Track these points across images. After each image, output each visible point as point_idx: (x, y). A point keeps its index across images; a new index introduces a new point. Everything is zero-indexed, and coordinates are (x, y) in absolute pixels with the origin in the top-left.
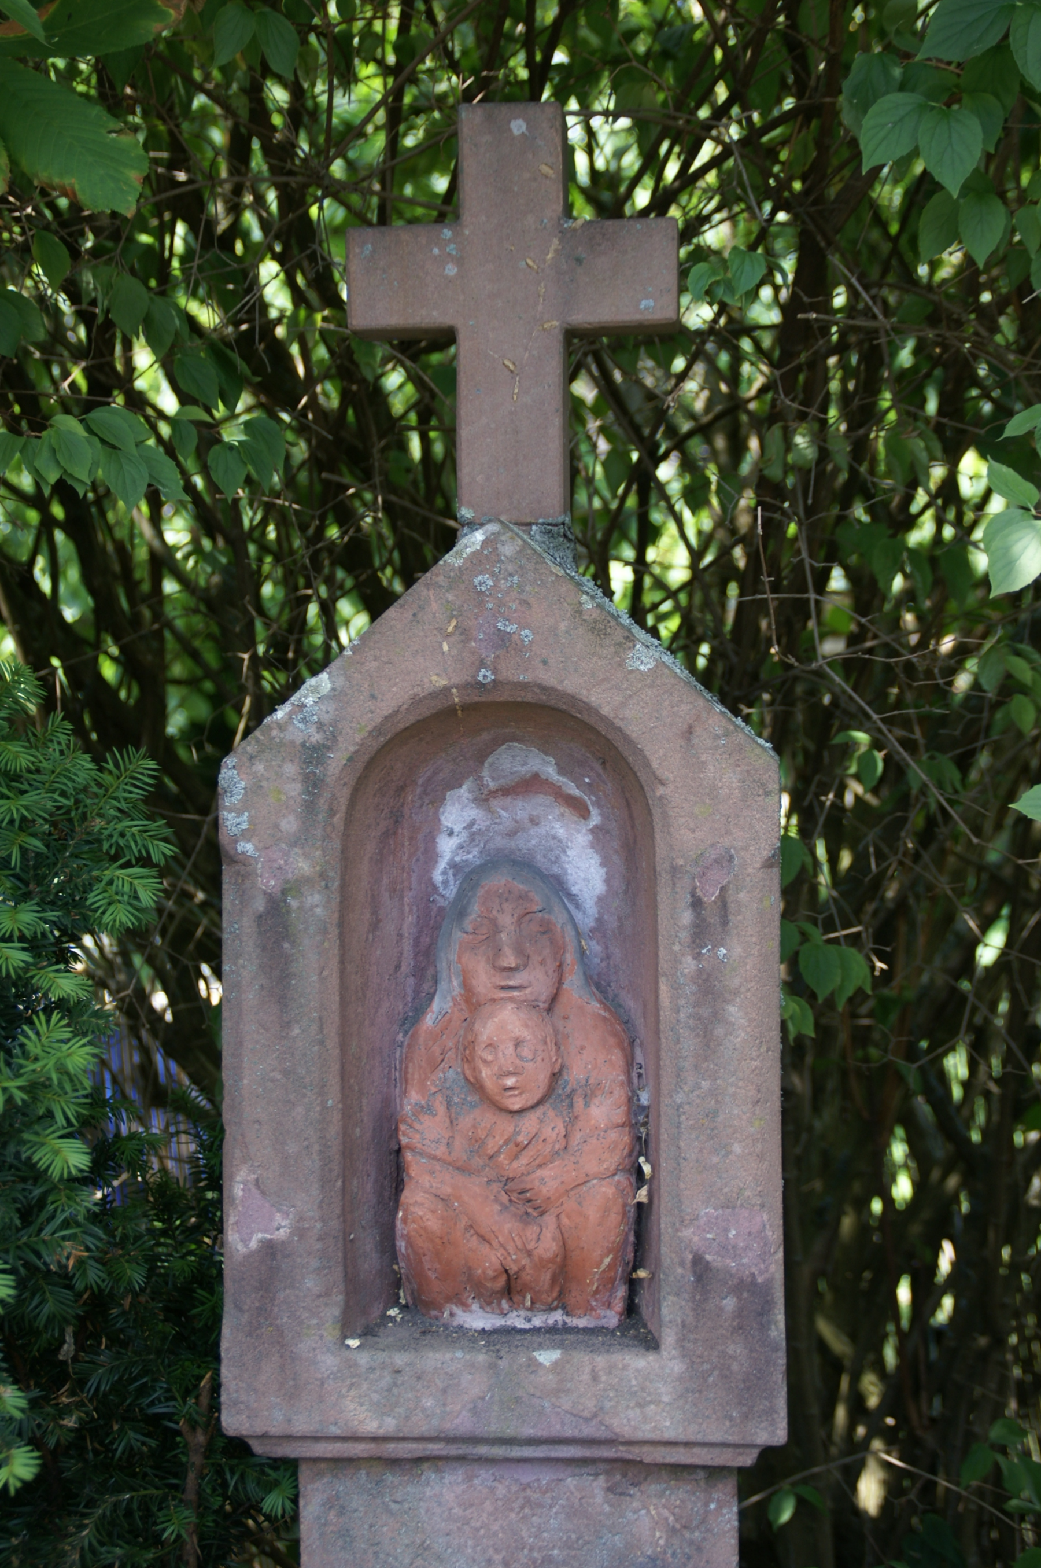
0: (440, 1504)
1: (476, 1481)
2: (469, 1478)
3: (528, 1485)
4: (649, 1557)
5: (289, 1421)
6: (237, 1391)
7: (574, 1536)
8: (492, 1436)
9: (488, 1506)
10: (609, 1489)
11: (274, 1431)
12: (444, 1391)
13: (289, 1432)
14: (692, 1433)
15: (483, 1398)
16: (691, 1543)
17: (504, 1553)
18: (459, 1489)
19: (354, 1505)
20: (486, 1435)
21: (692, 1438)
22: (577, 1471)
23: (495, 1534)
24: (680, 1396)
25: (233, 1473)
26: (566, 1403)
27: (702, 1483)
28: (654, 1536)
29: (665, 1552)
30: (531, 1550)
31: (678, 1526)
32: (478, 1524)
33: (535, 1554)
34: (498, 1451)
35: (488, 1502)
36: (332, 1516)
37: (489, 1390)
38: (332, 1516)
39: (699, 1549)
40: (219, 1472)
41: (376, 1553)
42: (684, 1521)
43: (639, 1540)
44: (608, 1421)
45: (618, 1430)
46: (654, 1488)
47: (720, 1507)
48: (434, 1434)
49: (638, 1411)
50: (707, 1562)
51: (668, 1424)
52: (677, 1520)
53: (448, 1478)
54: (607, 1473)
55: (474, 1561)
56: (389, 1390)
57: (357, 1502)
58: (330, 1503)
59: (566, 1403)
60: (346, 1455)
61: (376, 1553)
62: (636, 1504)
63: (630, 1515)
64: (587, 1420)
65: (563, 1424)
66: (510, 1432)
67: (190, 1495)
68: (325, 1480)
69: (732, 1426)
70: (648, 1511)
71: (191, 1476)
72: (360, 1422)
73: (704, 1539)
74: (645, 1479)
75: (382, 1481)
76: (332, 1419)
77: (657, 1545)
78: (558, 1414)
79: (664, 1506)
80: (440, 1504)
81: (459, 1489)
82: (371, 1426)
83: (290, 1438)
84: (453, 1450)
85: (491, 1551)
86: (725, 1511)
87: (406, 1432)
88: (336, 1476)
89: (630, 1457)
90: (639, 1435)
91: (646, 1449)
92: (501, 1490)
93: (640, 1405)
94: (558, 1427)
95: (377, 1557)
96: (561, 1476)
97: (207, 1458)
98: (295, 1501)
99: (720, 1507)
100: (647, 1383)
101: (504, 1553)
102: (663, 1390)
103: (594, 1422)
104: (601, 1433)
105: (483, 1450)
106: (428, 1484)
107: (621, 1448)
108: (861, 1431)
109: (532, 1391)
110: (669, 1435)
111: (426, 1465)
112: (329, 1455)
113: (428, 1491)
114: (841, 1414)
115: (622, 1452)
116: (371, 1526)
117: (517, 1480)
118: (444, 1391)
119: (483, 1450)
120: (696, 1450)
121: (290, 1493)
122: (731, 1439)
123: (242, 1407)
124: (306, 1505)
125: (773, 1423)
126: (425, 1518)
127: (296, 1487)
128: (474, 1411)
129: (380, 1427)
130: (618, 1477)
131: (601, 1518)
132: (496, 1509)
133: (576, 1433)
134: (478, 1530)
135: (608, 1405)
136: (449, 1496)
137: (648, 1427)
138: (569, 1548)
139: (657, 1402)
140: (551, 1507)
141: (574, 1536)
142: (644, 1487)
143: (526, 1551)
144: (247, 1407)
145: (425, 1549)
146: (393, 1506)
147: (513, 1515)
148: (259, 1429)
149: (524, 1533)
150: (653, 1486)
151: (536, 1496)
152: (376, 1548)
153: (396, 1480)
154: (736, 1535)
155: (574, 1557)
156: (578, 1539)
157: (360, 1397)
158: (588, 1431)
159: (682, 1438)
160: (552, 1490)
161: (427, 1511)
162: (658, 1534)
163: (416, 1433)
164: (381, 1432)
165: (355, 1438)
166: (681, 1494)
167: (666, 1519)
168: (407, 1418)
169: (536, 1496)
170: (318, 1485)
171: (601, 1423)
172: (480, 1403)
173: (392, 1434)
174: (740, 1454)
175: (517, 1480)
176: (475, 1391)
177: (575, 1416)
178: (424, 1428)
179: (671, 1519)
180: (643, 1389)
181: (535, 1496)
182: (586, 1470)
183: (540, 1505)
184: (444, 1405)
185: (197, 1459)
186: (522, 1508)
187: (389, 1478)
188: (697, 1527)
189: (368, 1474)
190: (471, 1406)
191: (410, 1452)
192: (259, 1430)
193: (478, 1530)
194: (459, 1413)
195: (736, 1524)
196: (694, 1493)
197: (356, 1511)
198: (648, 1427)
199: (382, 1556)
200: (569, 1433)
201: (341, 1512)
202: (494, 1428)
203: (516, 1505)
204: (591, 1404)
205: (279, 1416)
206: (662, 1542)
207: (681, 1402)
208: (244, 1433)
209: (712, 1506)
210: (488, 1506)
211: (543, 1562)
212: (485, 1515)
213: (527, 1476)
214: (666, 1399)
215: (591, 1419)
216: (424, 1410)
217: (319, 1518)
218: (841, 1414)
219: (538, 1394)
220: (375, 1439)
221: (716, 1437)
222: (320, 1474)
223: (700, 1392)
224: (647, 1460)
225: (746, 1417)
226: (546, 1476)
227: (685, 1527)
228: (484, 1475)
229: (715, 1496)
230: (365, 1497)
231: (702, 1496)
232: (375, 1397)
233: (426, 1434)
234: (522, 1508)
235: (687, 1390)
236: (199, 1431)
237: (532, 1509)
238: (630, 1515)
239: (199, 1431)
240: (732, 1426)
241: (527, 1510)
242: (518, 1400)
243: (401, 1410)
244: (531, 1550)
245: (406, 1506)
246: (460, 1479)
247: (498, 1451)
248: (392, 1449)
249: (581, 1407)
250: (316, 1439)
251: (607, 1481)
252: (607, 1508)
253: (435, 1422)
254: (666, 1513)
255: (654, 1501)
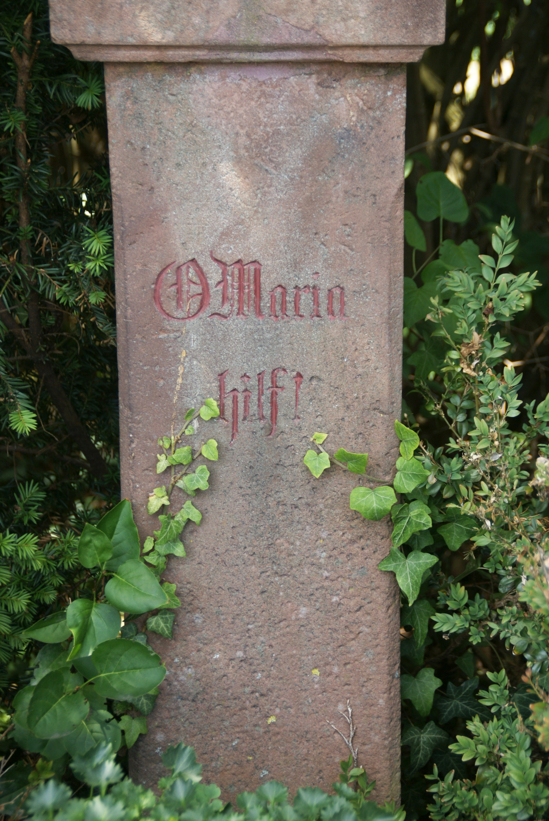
0: (203, 96)
1: (228, 80)
2: (223, 78)
3: (264, 82)
4: (345, 129)
5: (99, 33)
6: (61, 12)
7: (294, 117)
8: (241, 44)
9: (236, 97)
10: (319, 84)
11: (89, 41)
12: (208, 12)
13: (99, 42)
14: (379, 39)
15: (234, 17)
16: (374, 118)
17: (247, 128)
18: (216, 86)
19: (144, 97)
20: (237, 43)
21: (379, 42)
22: (297, 72)
23: (241, 116)
24: (372, 13)
25: (51, 85)
26: (293, 19)
27: (383, 79)
28: (349, 115)
29: (356, 126)
30: (265, 126)
31: (365, 108)
32: (230, 109)
33: (268, 129)
34: (245, 56)
35: (236, 94)
36: (129, 104)
37: (239, 11)
38: (129, 104)
39: (379, 123)
40: (42, 86)
41: (160, 130)
42: (369, 104)
43: (339, 118)
44: (321, 31)
45: (328, 38)
46: (350, 82)
47: (394, 94)
48: (201, 43)
49: (342, 24)
50: (384, 131)
51: (363, 32)
52: (364, 104)
53: (208, 78)
54: (318, 73)
55: (227, 134)
56: (169, 12)
57: (146, 95)
58: (127, 95)
59: (293, 19)
60: (139, 60)
61: (160, 130)
62: (337, 94)
63: (333, 101)
64: (307, 31)
65: (290, 34)
66: (254, 41)
67: (21, 103)
68: (123, 79)
69: (407, 33)
70: (346, 98)
71: (20, 89)
72: (149, 34)
73: (383, 116)
74: (344, 77)
75: (162, 80)
76: (129, 33)
77: (351, 121)
78: (287, 27)
79: (357, 95)
80: (203, 96)
81: (216, 86)
82: (157, 37)
83: (99, 46)
84: (213, 56)
85: (238, 127)
86: (397, 96)
87: (181, 42)
88: (131, 77)
89: (336, 58)
90: (344, 41)
91: (347, 52)
92: (245, 86)
93: (344, 20)
94: (287, 36)
95: (161, 132)
96: (287, 75)
97: (30, 77)
98: (102, 96)
99: (394, 94)
100: (349, 4)
101: (247, 128)
102: (360, 8)
103: (312, 33)
104: (317, 41)
105: (234, 56)
106: (195, 83)
107: (329, 52)
108: (445, 146)
109: (269, 11)
110: (364, 40)
111: (193, 69)
112: (127, 60)
113: (195, 87)
114: (433, 130)
115: (330, 55)
116: (156, 111)
117: (256, 79)
118: (208, 12)
119: (234, 56)
120: (382, 52)
121: (97, 91)
122: (406, 41)
123: (65, 23)
124: (111, 96)
125: (436, 29)
126: (193, 106)
127: (103, 88)
128: (229, 26)
129: (163, 38)
130: (326, 75)
131: (314, 104)
132: (242, 99)
133: (300, 41)
134: (229, 113)
135: (322, 20)
136: (209, 91)
137: (349, 35)
138: (291, 125)
139: (356, 17)
140: (279, 97)
141: (294, 117)
142: (343, 82)
143: (262, 127)
144: (69, 23)
145: (193, 127)
146: (171, 98)
147: (253, 103)
148: (78, 39)
149: (261, 115)
150: (349, 81)
151: (269, 89)
152: (161, 126)
153: (173, 80)
154: (405, 112)
155: (294, 130)
156: (297, 119)
157: (148, 17)
158: (308, 39)
159: (373, 42)
160: (280, 86)
161: (194, 100)
162: (352, 113)
163: (188, 43)
164: (164, 41)
165: (146, 47)
166: (368, 86)
167: (358, 103)
168: (182, 31)
169: (269, 89)
170: (118, 83)
171: (317, 33)
172: (233, 20)
173: (172, 43)
174: (411, 54)
175: (256, 79)
176: (229, 12)
177: (298, 28)
178: (192, 38)
179: (361, 103)
180: (346, 8)
181: (268, 90)
182: (304, 71)
183: (272, 96)
184: (208, 22)
185: (24, 78)
186: (259, 98)
187: (168, 78)
188: (378, 108)
189: (153, 75)
190: (227, 22)
191: (183, 57)
192: (78, 40)
193: (229, 113)
194: (218, 28)
195: (405, 105)
196: (377, 85)
197: (145, 100)
198: (349, 35)
199: (163, 131)
200: (294, 40)
201: (135, 102)
202: (243, 38)
203: (255, 97)
204: (310, 20)
205: (91, 30)
206: (354, 119)
207: (372, 17)
208: (68, 42)
209: (389, 93)
210: (236, 97)
211: (273, 134)
212: (234, 103)
213: (263, 74)
214: (362, 15)
215: (310, 31)
216: (193, 26)
217: (120, 105)
218: (433, 130)
219: (273, 13)
220: (159, 47)
221: (396, 40)
222: (120, 76)
223: (386, 9)
224: (347, 60)
225: (417, 26)
226: (275, 75)
227: (370, 108)
228: (233, 75)
229: (391, 86)
230: (151, 91)
231: (382, 87)
232: (159, 16)
233: (196, 43)
234: (259, 98)
235: (377, 8)
236: (25, 56)
237: (266, 99)
238: (333, 101)
239: (25, 56)
240: (407, 33)
241: (262, 100)
242: (259, 18)
243: (177, 26)
244: (265, 126)
245: (180, 97)
246: (217, 79)
247: (245, 56)
248: (171, 55)
249: (303, 22)
250: (118, 47)
251: (318, 78)
252: (317, 97)
253: (202, 34)
254: (357, 99)
255: (350, 91)
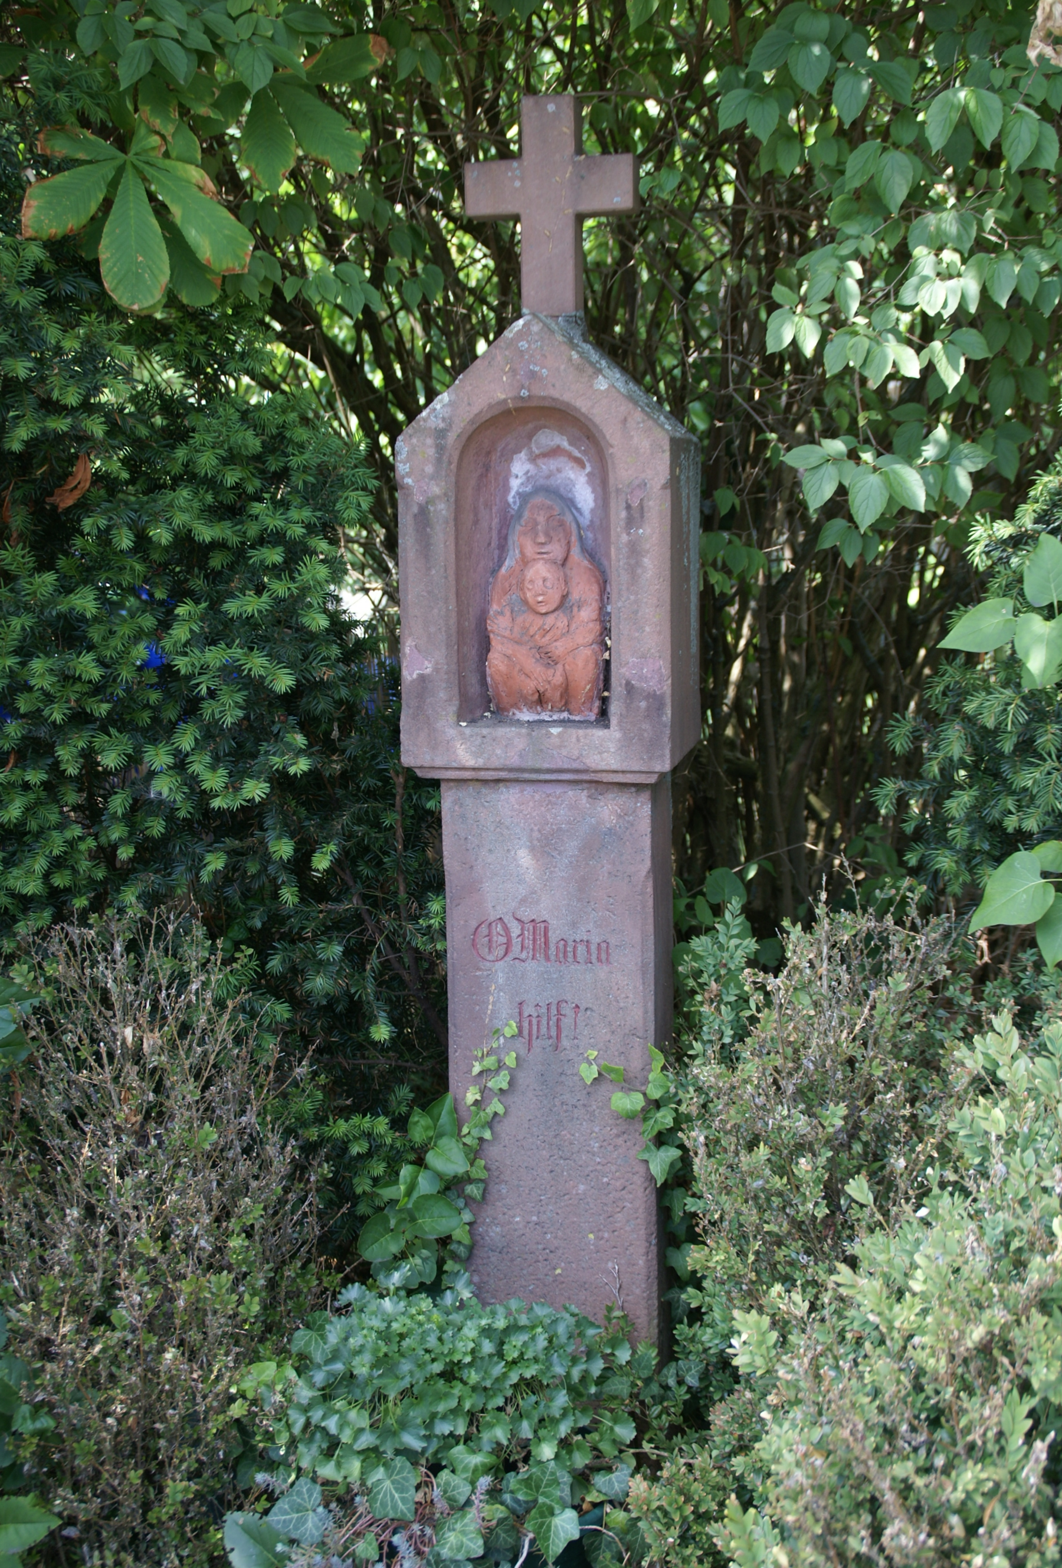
26: (564, 752)
34: (534, 776)
40: (410, 796)
46: (610, 796)
57: (468, 801)
58: (456, 802)
59: (564, 752)
66: (538, 766)
67: (398, 808)
82: (471, 763)
84: (512, 775)
92: (537, 797)
104: (581, 767)
105: (526, 776)
110: (614, 767)
128: (521, 756)
136: (512, 800)
158: (575, 765)
178: (496, 763)
202: (530, 764)
204: (576, 753)
213: (549, 789)
226: (559, 790)
228: (529, 789)
248: (483, 775)
